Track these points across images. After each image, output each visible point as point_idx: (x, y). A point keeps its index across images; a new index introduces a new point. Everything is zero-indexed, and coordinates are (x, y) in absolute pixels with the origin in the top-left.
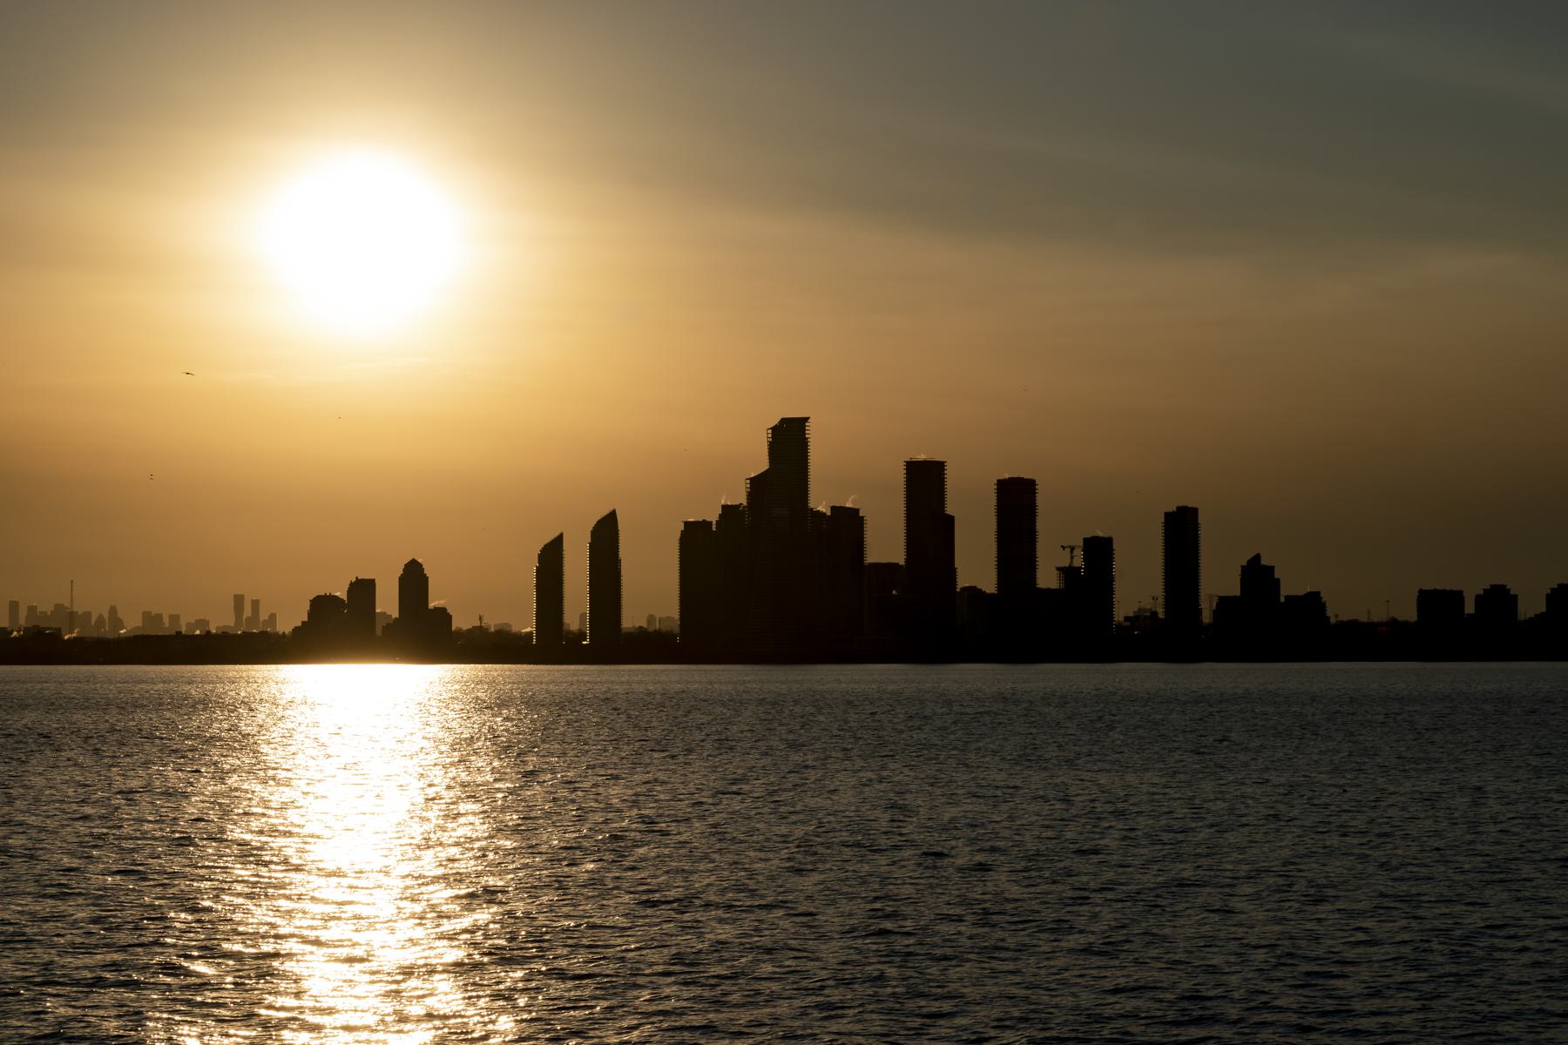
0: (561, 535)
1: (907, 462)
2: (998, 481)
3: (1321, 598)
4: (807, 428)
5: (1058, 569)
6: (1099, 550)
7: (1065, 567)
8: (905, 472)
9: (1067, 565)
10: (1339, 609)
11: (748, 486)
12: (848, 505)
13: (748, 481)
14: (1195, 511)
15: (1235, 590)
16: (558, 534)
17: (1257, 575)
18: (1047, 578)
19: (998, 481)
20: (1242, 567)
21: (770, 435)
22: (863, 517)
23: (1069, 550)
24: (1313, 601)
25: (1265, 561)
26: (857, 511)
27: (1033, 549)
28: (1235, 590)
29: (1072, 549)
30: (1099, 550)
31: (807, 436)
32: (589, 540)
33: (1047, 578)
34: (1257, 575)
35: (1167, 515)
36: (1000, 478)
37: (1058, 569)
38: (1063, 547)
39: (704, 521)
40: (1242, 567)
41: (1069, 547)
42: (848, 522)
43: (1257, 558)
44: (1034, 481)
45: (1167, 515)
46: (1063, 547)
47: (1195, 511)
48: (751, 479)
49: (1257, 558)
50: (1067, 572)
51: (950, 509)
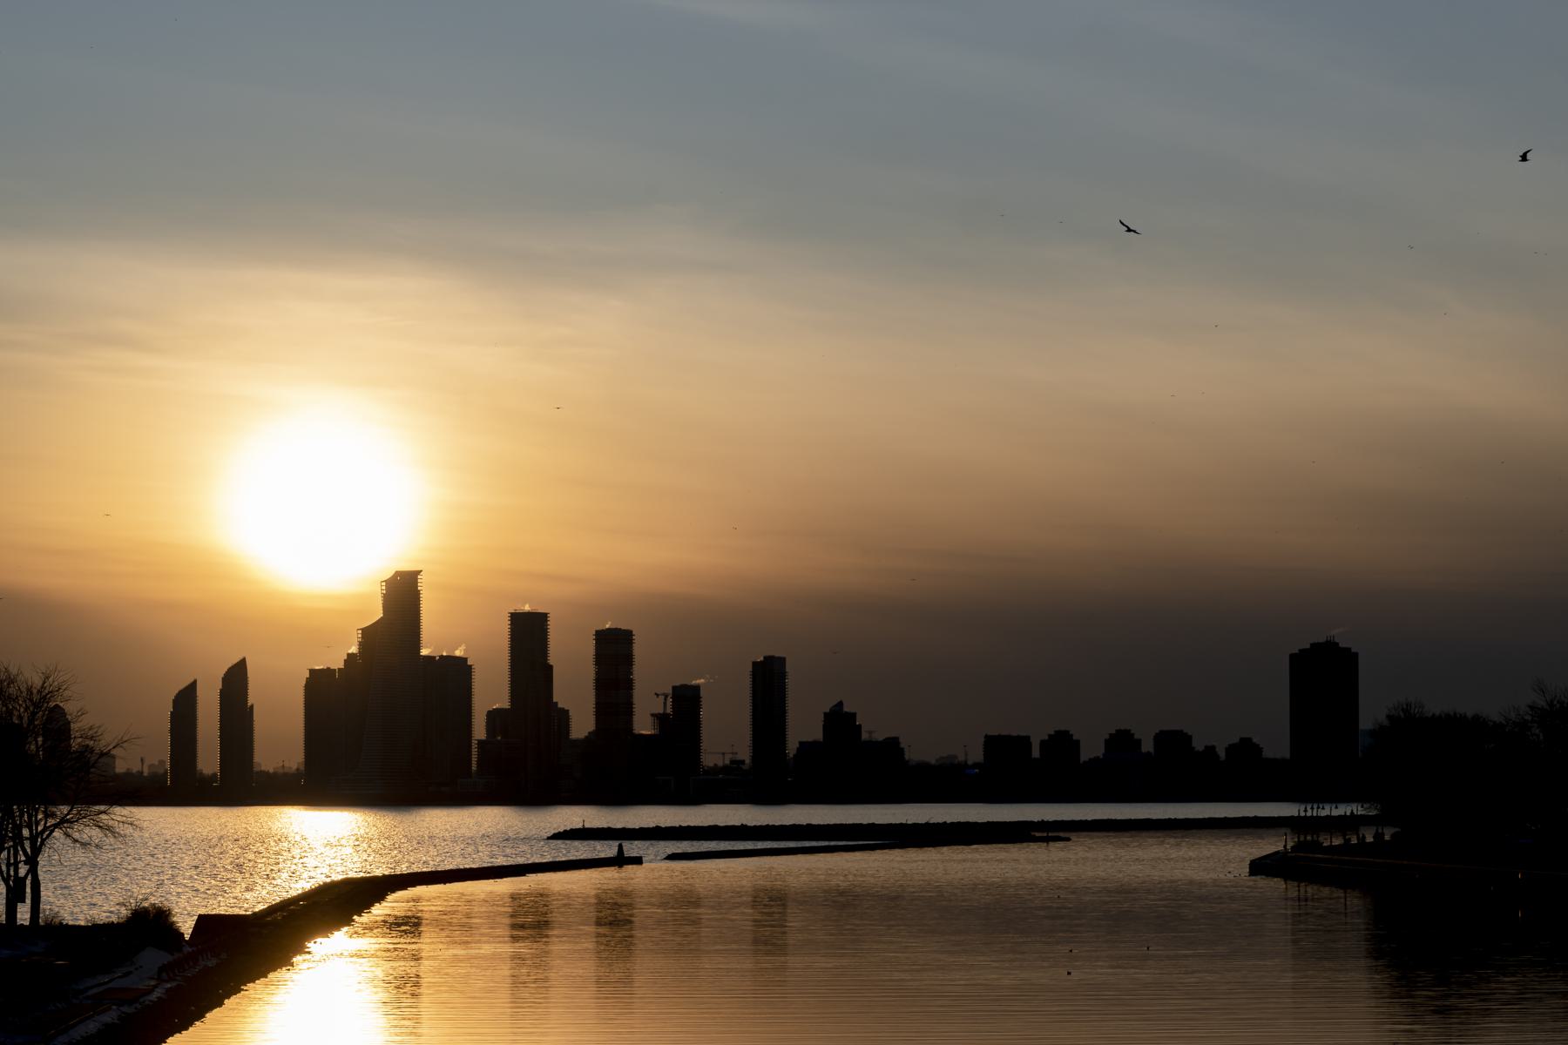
0: (193, 685)
1: (511, 613)
2: (597, 631)
3: (898, 743)
4: (419, 581)
5: (652, 715)
6: (686, 700)
7: (660, 714)
8: (509, 622)
9: (662, 712)
10: (915, 752)
11: (360, 636)
12: (458, 653)
13: (360, 632)
14: (782, 660)
15: (816, 733)
16: (192, 680)
17: (839, 721)
18: (643, 725)
19: (597, 631)
20: (825, 714)
21: (384, 588)
22: (471, 666)
23: (663, 697)
24: (893, 744)
25: (846, 709)
26: (466, 659)
27: (631, 696)
28: (816, 733)
29: (666, 696)
30: (686, 700)
31: (419, 588)
32: (220, 687)
33: (643, 725)
34: (839, 721)
35: (755, 664)
36: (600, 628)
37: (652, 715)
38: (657, 695)
39: (328, 668)
40: (825, 714)
41: (663, 694)
42: (456, 671)
43: (840, 704)
44: (631, 632)
45: (755, 664)
46: (657, 695)
47: (782, 660)
48: (364, 630)
49: (840, 704)
50: (660, 719)
51: (552, 660)
